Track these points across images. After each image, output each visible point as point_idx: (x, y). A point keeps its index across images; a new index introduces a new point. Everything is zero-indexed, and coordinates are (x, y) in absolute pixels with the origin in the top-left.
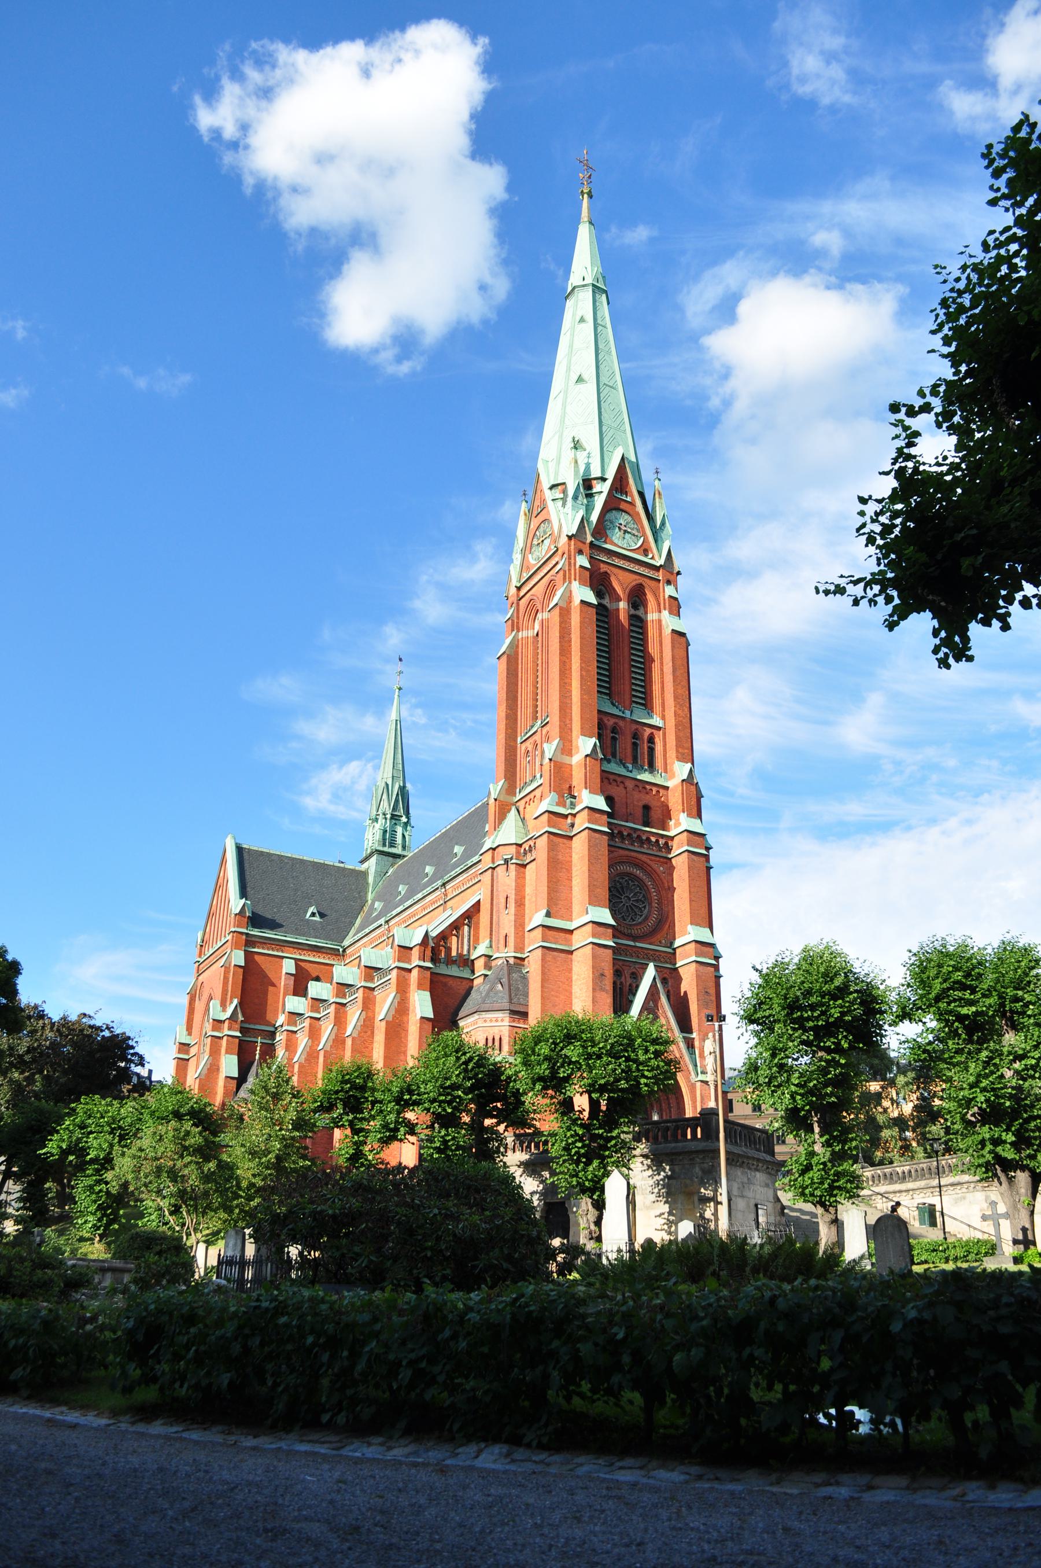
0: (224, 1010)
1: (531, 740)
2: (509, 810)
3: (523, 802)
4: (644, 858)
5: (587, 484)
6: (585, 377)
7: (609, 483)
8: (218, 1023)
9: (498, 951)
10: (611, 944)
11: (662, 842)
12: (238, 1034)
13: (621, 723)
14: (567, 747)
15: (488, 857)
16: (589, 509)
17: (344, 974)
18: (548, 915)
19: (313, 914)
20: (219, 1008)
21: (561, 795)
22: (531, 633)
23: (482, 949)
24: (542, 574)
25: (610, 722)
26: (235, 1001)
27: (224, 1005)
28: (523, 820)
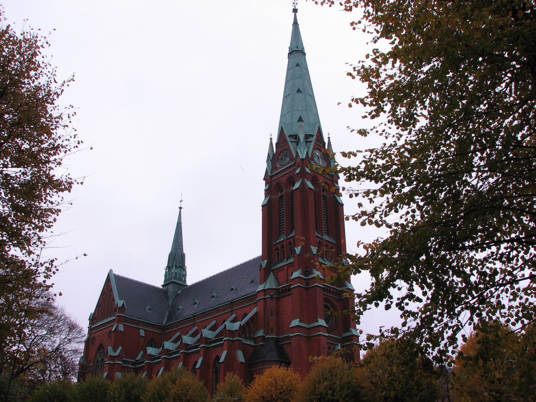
0: (115, 351)
1: (281, 244)
2: (270, 274)
3: (276, 271)
4: (331, 299)
5: (307, 137)
6: (301, 90)
7: (315, 137)
8: (112, 358)
9: (268, 335)
10: (327, 335)
11: (338, 292)
12: (121, 363)
13: (321, 241)
14: (306, 249)
15: (262, 293)
16: (308, 148)
17: (187, 340)
18: (300, 321)
19: (149, 309)
20: (112, 350)
21: (302, 270)
22: (277, 197)
23: (260, 333)
24: (287, 172)
25: (318, 240)
26: (120, 348)
27: (115, 350)
28: (276, 278)
